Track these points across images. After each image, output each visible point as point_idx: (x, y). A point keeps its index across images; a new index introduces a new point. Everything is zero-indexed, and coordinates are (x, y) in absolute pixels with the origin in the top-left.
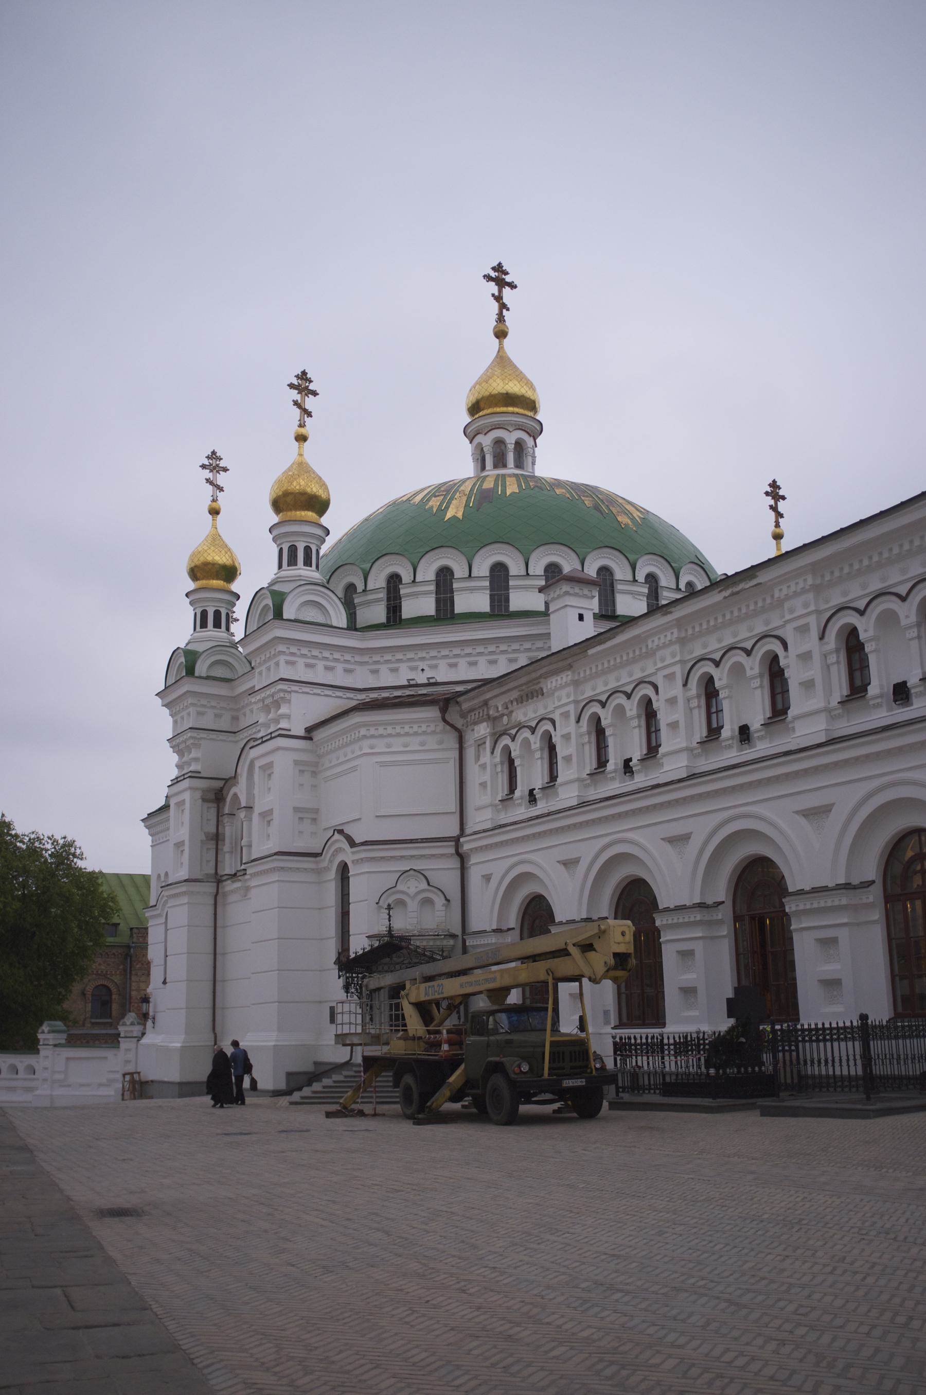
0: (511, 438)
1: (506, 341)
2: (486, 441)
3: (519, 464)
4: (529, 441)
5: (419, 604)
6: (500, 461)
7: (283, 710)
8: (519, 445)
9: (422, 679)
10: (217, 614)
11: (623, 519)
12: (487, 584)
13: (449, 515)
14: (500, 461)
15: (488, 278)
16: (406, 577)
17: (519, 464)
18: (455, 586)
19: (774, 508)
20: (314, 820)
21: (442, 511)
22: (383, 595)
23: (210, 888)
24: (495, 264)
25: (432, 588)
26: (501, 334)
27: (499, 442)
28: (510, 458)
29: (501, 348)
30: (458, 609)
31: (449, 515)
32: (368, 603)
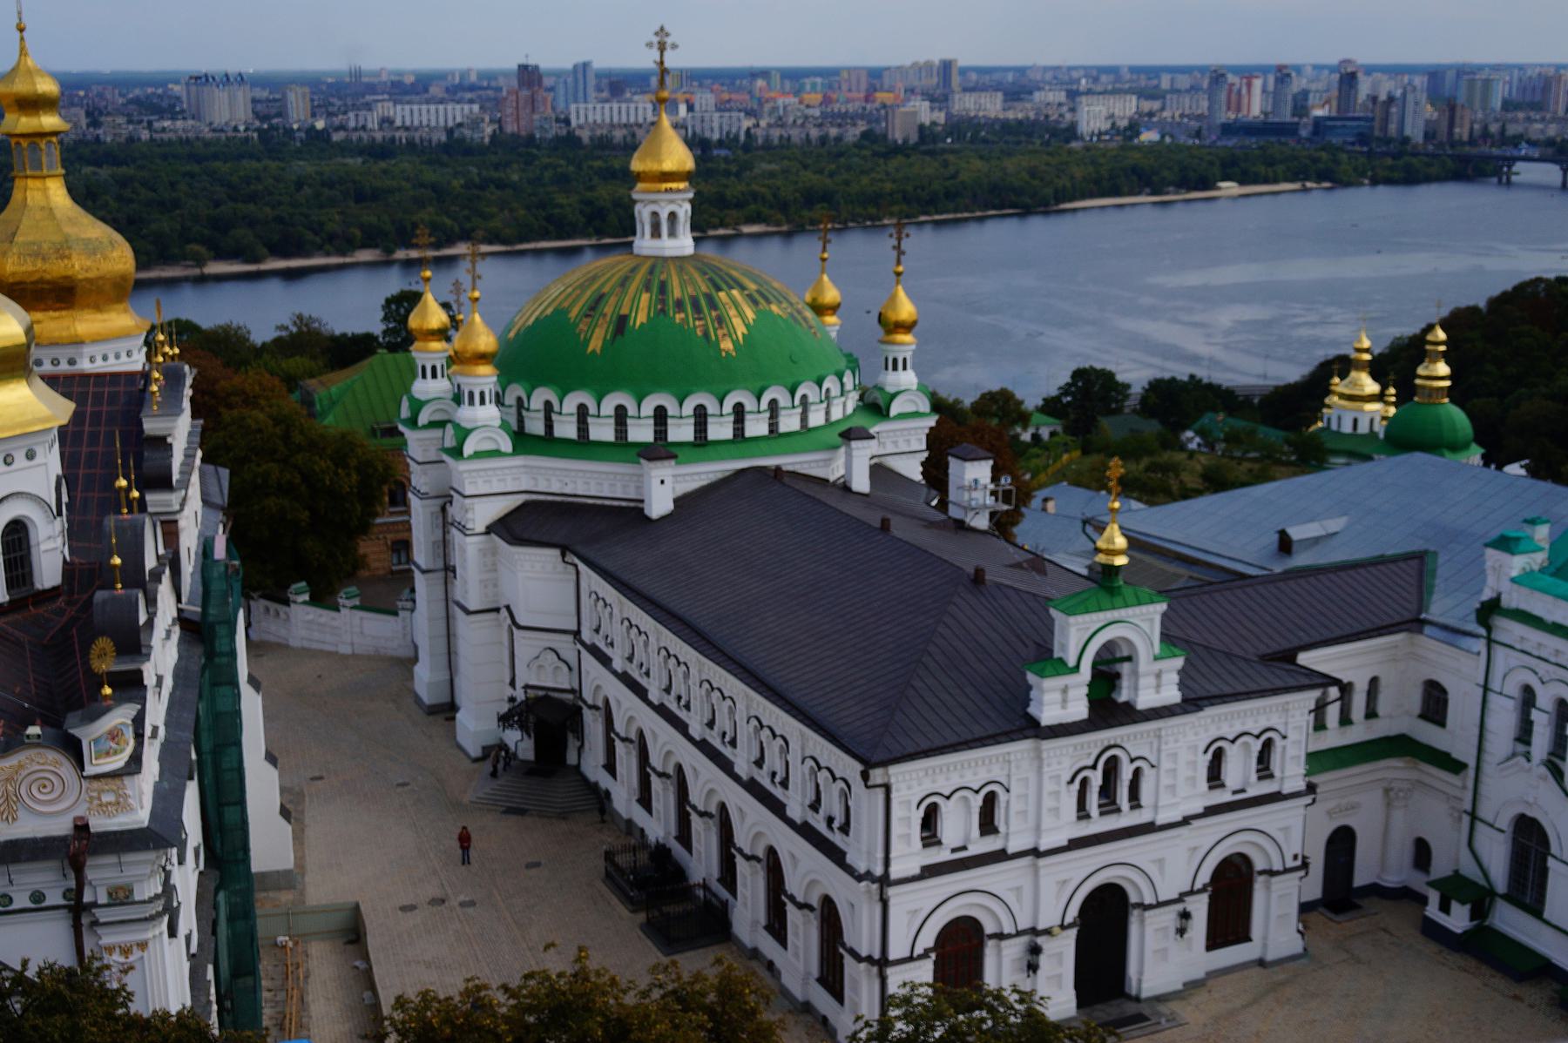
7: (470, 515)
9: (568, 490)
10: (434, 368)
11: (727, 345)
13: (590, 349)
15: (650, 45)
16: (556, 408)
18: (590, 420)
19: (898, 248)
20: (495, 586)
21: (587, 341)
22: (541, 415)
23: (442, 574)
24: (657, 28)
25: (575, 418)
27: (655, 214)
31: (590, 349)
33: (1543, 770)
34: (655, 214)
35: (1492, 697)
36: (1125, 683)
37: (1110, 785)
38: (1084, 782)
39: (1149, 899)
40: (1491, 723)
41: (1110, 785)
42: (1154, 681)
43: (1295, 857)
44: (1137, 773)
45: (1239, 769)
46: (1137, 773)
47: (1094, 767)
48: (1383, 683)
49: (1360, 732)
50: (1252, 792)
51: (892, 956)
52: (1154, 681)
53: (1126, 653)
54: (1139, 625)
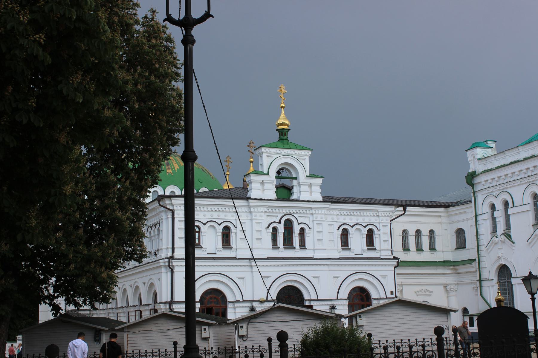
33: (503, 237)
35: (479, 218)
36: (295, 190)
37: (288, 234)
38: (275, 230)
39: (314, 296)
40: (481, 230)
41: (288, 234)
42: (308, 189)
43: (392, 293)
44: (302, 230)
45: (358, 242)
46: (302, 230)
47: (279, 223)
48: (437, 233)
49: (426, 256)
50: (365, 255)
51: (176, 299)
52: (308, 189)
53: (294, 176)
54: (300, 161)
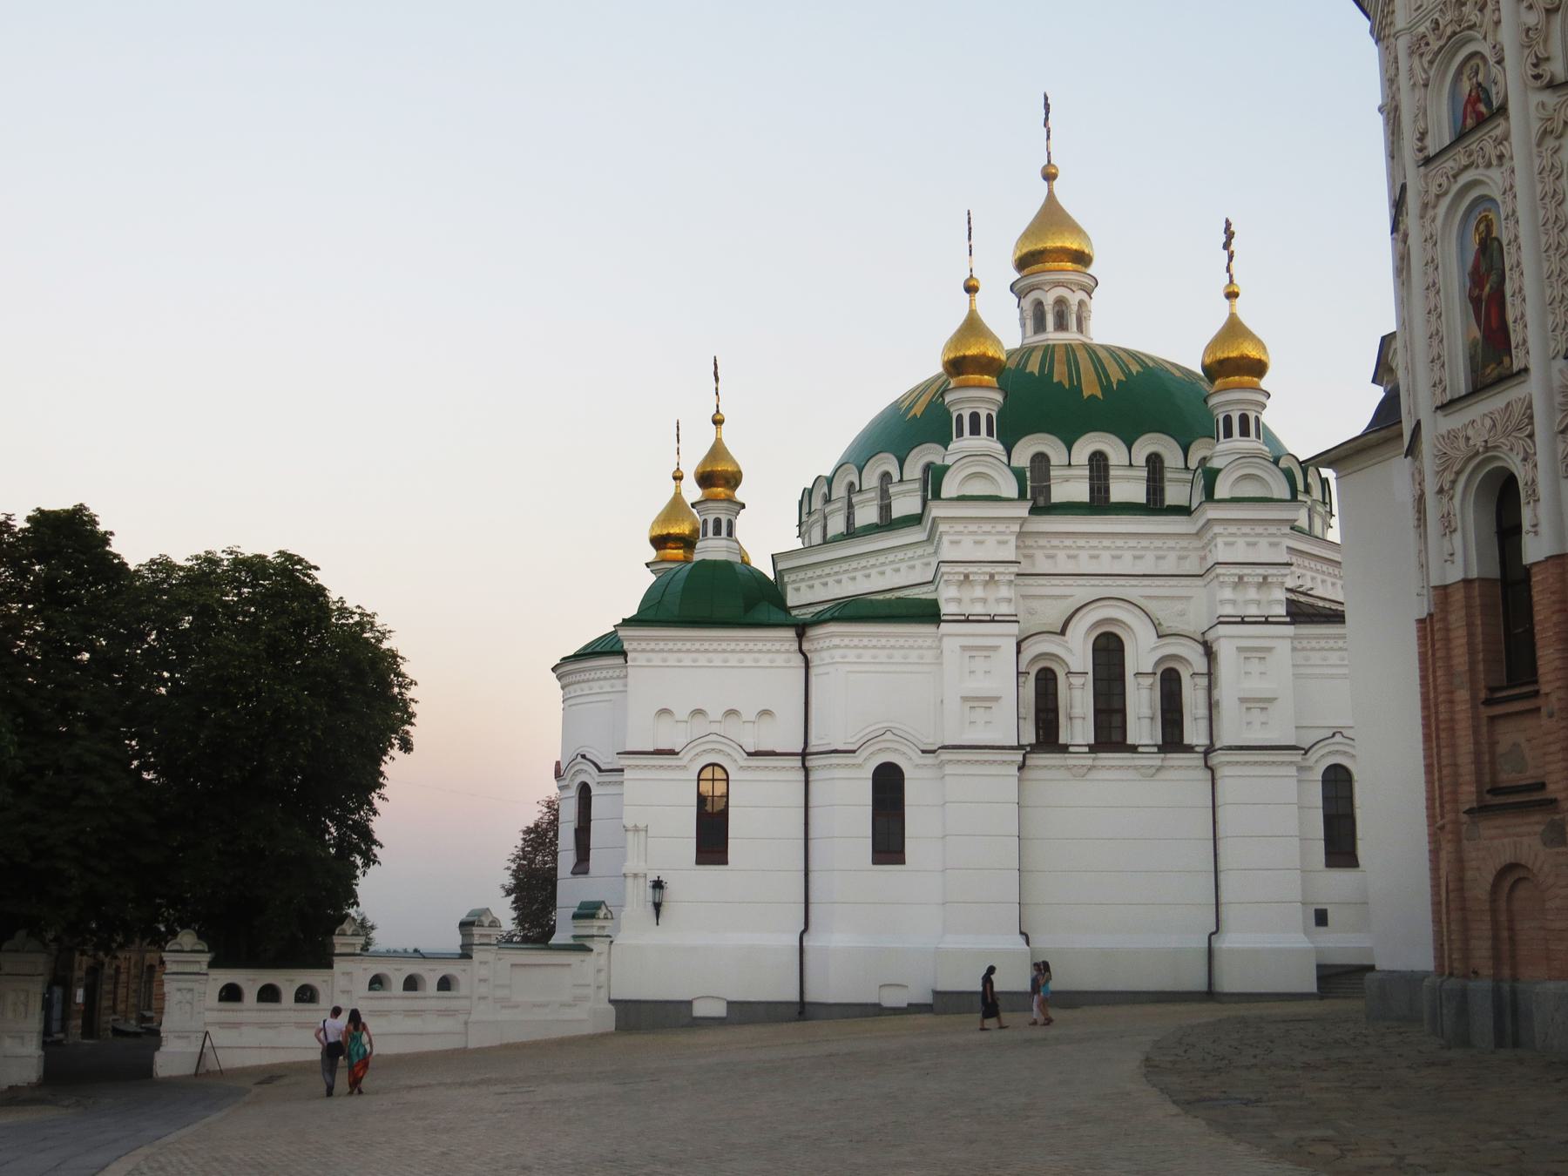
0: (1049, 299)
1: (1055, 183)
2: (1027, 303)
3: (1061, 325)
4: (1074, 298)
5: (867, 514)
6: (1040, 326)
8: (1061, 302)
11: (1091, 388)
12: (917, 485)
14: (1040, 326)
17: (1061, 325)
18: (892, 490)
26: (1049, 176)
28: (1050, 320)
29: (1051, 196)
30: (895, 514)
32: (832, 512)
34: (1039, 304)
